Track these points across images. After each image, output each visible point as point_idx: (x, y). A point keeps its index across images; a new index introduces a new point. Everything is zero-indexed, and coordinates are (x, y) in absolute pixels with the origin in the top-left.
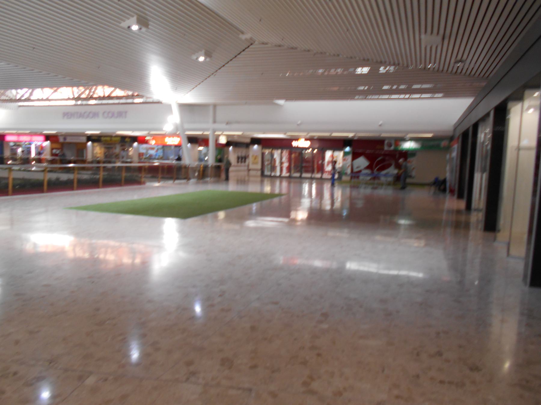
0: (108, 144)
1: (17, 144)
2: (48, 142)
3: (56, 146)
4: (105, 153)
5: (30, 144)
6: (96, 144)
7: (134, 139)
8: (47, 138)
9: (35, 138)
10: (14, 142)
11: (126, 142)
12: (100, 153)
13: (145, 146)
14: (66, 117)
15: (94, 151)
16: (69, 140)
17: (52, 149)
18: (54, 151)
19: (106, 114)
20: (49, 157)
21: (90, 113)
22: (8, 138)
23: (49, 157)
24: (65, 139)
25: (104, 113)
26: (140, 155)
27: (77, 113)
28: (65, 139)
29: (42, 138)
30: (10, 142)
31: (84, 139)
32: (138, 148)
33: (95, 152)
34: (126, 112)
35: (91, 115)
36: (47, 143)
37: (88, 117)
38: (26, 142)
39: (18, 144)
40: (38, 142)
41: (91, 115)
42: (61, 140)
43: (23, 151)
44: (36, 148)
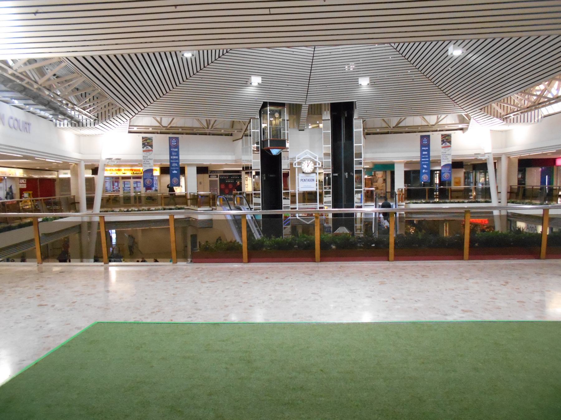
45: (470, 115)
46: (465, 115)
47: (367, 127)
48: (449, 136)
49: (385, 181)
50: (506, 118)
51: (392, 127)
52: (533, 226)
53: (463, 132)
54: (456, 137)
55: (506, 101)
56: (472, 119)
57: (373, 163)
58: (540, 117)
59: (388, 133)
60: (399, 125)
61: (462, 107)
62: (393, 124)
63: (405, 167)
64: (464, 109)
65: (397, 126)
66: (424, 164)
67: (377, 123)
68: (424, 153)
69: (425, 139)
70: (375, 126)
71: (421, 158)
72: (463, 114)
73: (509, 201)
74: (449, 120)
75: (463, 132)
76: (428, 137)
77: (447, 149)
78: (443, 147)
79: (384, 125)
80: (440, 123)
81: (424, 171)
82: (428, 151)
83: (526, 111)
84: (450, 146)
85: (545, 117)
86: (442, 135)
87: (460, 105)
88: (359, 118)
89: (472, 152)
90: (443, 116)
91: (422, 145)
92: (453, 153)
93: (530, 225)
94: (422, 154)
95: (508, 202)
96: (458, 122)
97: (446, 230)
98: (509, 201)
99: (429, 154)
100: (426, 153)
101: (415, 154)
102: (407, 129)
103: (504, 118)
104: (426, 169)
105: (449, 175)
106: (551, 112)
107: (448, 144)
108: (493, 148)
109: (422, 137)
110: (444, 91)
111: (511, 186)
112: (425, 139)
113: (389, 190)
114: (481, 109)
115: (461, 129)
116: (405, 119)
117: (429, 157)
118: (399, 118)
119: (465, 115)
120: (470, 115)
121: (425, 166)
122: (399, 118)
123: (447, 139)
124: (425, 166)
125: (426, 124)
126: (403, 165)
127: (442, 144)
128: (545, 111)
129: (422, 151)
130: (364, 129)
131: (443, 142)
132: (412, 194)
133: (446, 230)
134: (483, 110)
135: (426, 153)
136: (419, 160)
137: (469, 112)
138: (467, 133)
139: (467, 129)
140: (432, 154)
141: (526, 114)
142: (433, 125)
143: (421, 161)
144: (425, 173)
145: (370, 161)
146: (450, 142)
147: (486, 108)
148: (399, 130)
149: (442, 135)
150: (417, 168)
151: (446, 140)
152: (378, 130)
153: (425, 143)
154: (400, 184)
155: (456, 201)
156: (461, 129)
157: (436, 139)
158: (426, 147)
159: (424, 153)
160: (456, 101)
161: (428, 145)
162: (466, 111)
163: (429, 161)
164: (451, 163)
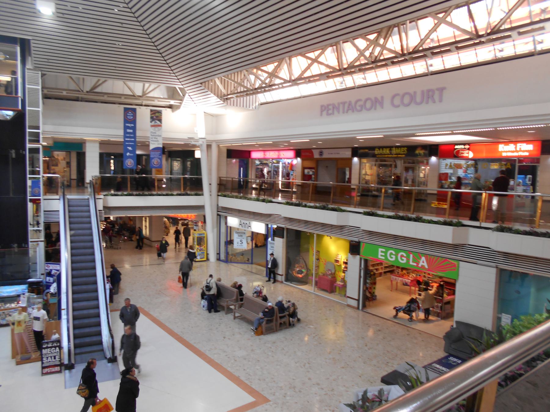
0: (381, 161)
1: (263, 163)
2: (299, 159)
3: (308, 164)
4: (378, 175)
5: (278, 162)
6: (364, 160)
7: (433, 149)
8: (298, 153)
9: (284, 154)
10: (259, 159)
11: (416, 155)
12: (371, 175)
13: (449, 161)
14: (325, 113)
15: (363, 171)
16: (326, 155)
17: (304, 168)
18: (306, 171)
19: (397, 101)
20: (299, 181)
21: (367, 100)
22: (254, 155)
23: (299, 181)
24: (321, 153)
25: (394, 97)
26: (443, 177)
27: (344, 103)
28: (321, 153)
29: (291, 154)
30: (255, 159)
31: (347, 154)
32: (438, 165)
33: (363, 172)
34: (441, 90)
35: (368, 105)
36: (298, 161)
37: (363, 107)
38: (273, 159)
39: (265, 162)
40: (288, 158)
41: (368, 105)
42: (316, 155)
43: (269, 172)
44: (284, 167)
45: (186, 89)
46: (179, 88)
47: (47, 86)
48: (160, 112)
49: (69, 164)
50: (227, 99)
51: (85, 91)
52: (248, 222)
53: (173, 111)
54: (166, 114)
55: (230, 77)
56: (187, 95)
57: (53, 138)
58: (257, 104)
59: (77, 100)
60: (96, 90)
61: (179, 77)
62: (87, 88)
63: (100, 148)
64: (181, 80)
65: (91, 91)
66: (129, 146)
67: (63, 82)
68: (128, 131)
69: (130, 113)
70: (58, 87)
71: (125, 137)
72: (177, 87)
73: (220, 194)
74: (157, 92)
75: (173, 111)
76: (134, 110)
77: (157, 129)
78: (152, 126)
79: (73, 86)
80: (148, 95)
81: (128, 154)
82: (134, 128)
83: (243, 96)
84: (160, 126)
85: (262, 104)
86: (151, 111)
87: (177, 74)
88: (36, 68)
89: (185, 136)
90: (153, 86)
91: (126, 121)
92: (164, 135)
93: (243, 221)
94: (125, 132)
95: (218, 195)
96: (166, 97)
97: (146, 226)
98: (220, 194)
99: (134, 133)
100: (131, 131)
101: (115, 132)
102: (105, 98)
103: (225, 98)
104: (130, 152)
105: (159, 161)
106: (269, 100)
107: (158, 123)
108: (206, 134)
109: (126, 109)
110: (161, 51)
111: (220, 178)
112: (130, 113)
113: (74, 176)
114: (201, 83)
115: (170, 107)
116: (105, 81)
117: (135, 137)
118: (95, 79)
119: (179, 88)
120: (186, 89)
121: (130, 148)
122: (95, 79)
123: (157, 117)
124: (130, 148)
125: (131, 94)
126: (97, 145)
127: (151, 122)
128: (262, 97)
129: (126, 128)
130: (43, 88)
131: (152, 119)
132: (106, 184)
133: (146, 226)
134: (203, 84)
135: (131, 131)
136: (122, 140)
137: (185, 86)
138: (178, 112)
139: (178, 107)
140: (138, 133)
141: (251, 97)
142: (140, 96)
143: (125, 141)
144: (130, 157)
145: (49, 136)
146: (160, 120)
147: (207, 83)
148: (94, 97)
149: (151, 111)
150: (120, 150)
151: (156, 117)
152: (64, 93)
153: (130, 118)
154: (92, 171)
155: (164, 193)
156: (170, 107)
157: (143, 115)
158: (131, 123)
159: (128, 131)
160: (172, 68)
161: (134, 121)
162: (183, 83)
163: (135, 142)
164: (161, 146)
